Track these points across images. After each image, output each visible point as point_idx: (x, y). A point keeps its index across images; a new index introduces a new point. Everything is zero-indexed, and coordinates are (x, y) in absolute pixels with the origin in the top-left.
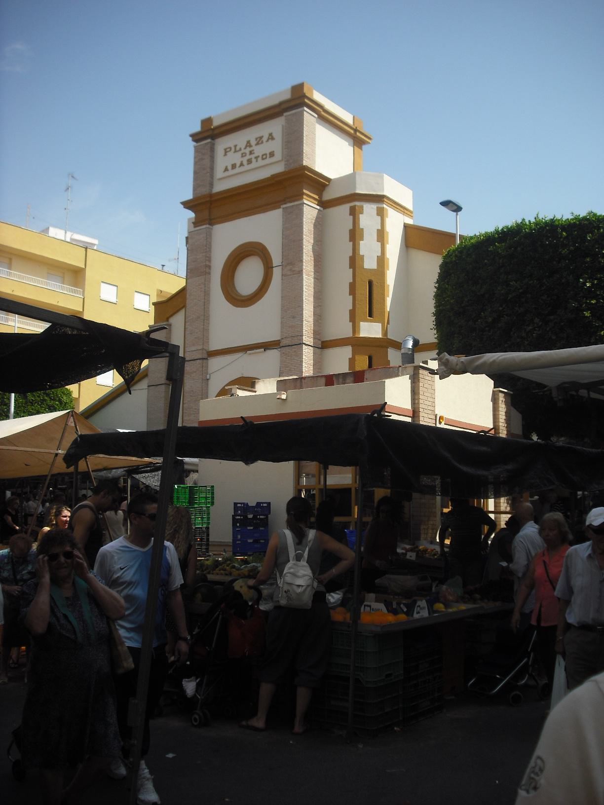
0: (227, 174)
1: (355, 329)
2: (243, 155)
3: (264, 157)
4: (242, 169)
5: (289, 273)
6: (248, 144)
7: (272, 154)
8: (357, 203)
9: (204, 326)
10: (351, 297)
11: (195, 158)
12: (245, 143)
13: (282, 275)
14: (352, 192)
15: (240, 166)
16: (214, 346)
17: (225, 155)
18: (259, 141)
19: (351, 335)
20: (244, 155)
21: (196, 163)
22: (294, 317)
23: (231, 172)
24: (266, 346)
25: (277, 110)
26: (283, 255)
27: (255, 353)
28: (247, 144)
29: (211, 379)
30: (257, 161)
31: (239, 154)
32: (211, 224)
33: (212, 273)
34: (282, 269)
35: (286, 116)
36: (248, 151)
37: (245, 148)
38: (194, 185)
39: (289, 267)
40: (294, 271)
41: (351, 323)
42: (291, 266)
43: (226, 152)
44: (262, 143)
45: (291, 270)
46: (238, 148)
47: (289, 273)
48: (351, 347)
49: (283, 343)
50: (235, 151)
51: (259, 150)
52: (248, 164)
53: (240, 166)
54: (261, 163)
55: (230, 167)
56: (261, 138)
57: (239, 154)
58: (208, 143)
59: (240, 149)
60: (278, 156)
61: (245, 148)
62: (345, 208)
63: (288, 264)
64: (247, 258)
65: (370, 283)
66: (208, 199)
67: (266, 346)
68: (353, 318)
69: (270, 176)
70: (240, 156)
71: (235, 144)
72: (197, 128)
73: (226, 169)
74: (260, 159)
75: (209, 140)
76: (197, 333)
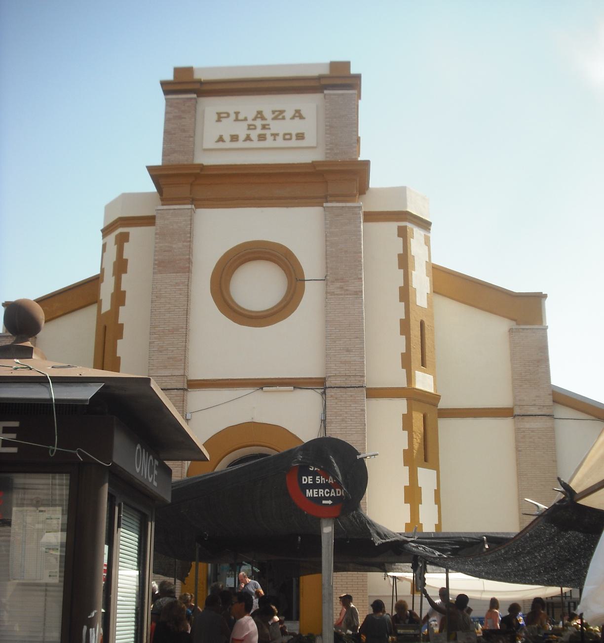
0: (221, 145)
1: (410, 378)
2: (251, 127)
3: (287, 137)
4: (248, 144)
5: (338, 291)
6: (260, 115)
7: (300, 136)
8: (409, 225)
9: (186, 343)
10: (403, 338)
11: (167, 113)
12: (255, 113)
13: (327, 293)
14: (404, 210)
15: (245, 140)
16: (197, 373)
17: (219, 120)
18: (279, 115)
19: (405, 385)
20: (251, 127)
21: (167, 121)
22: (348, 351)
23: (228, 144)
24: (297, 384)
25: (313, 84)
26: (327, 267)
27: (279, 391)
28: (257, 115)
29: (191, 420)
30: (275, 140)
31: (244, 125)
32: (197, 207)
33: (194, 270)
34: (327, 285)
35: (325, 95)
36: (259, 123)
37: (255, 119)
38: (164, 148)
39: (338, 284)
40: (347, 290)
41: (405, 370)
42: (342, 284)
43: (220, 117)
44: (284, 118)
45: (341, 288)
46: (241, 117)
47: (338, 291)
48: (406, 401)
49: (517, 411)
50: (237, 120)
51: (277, 127)
52: (297, 139)
53: (245, 140)
54: (280, 142)
55: (227, 138)
56: (282, 112)
57: (244, 125)
58: (191, 99)
59: (246, 119)
60: (311, 140)
61: (255, 119)
62: (393, 227)
63: (336, 280)
64: (249, 262)
65: (422, 324)
66: (198, 171)
67: (297, 384)
68: (406, 361)
69: (311, 162)
70: (246, 127)
71: (237, 110)
72: (170, 76)
73: (221, 139)
74: (280, 139)
75: (195, 96)
76: (173, 351)
